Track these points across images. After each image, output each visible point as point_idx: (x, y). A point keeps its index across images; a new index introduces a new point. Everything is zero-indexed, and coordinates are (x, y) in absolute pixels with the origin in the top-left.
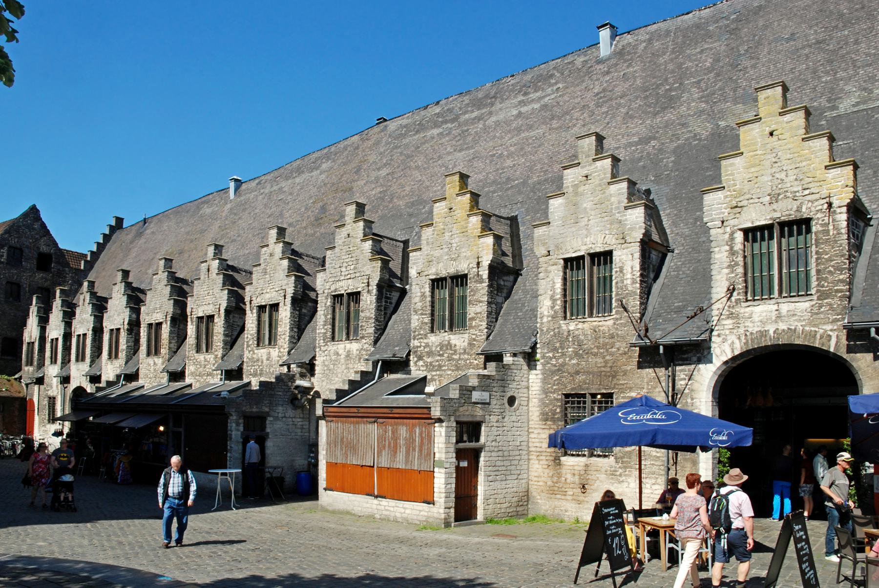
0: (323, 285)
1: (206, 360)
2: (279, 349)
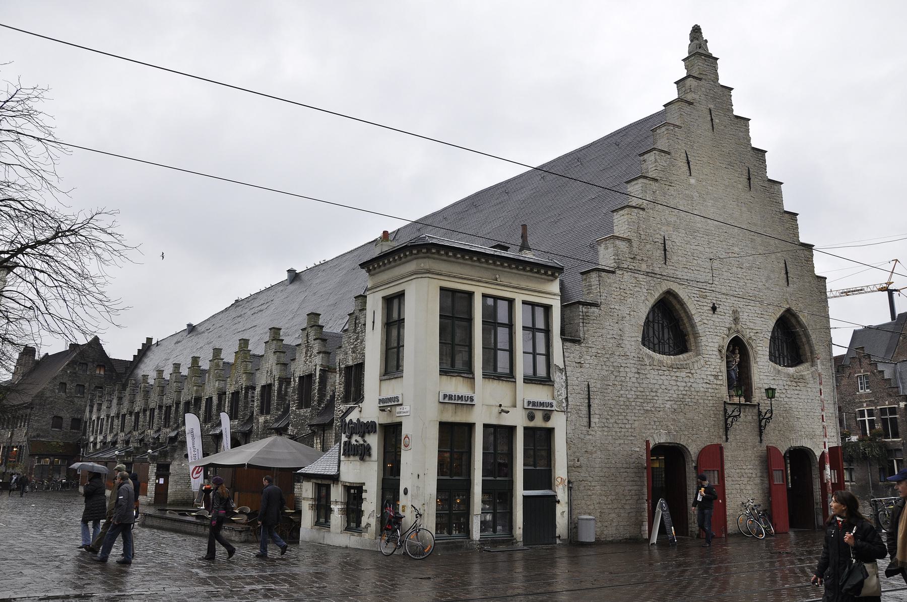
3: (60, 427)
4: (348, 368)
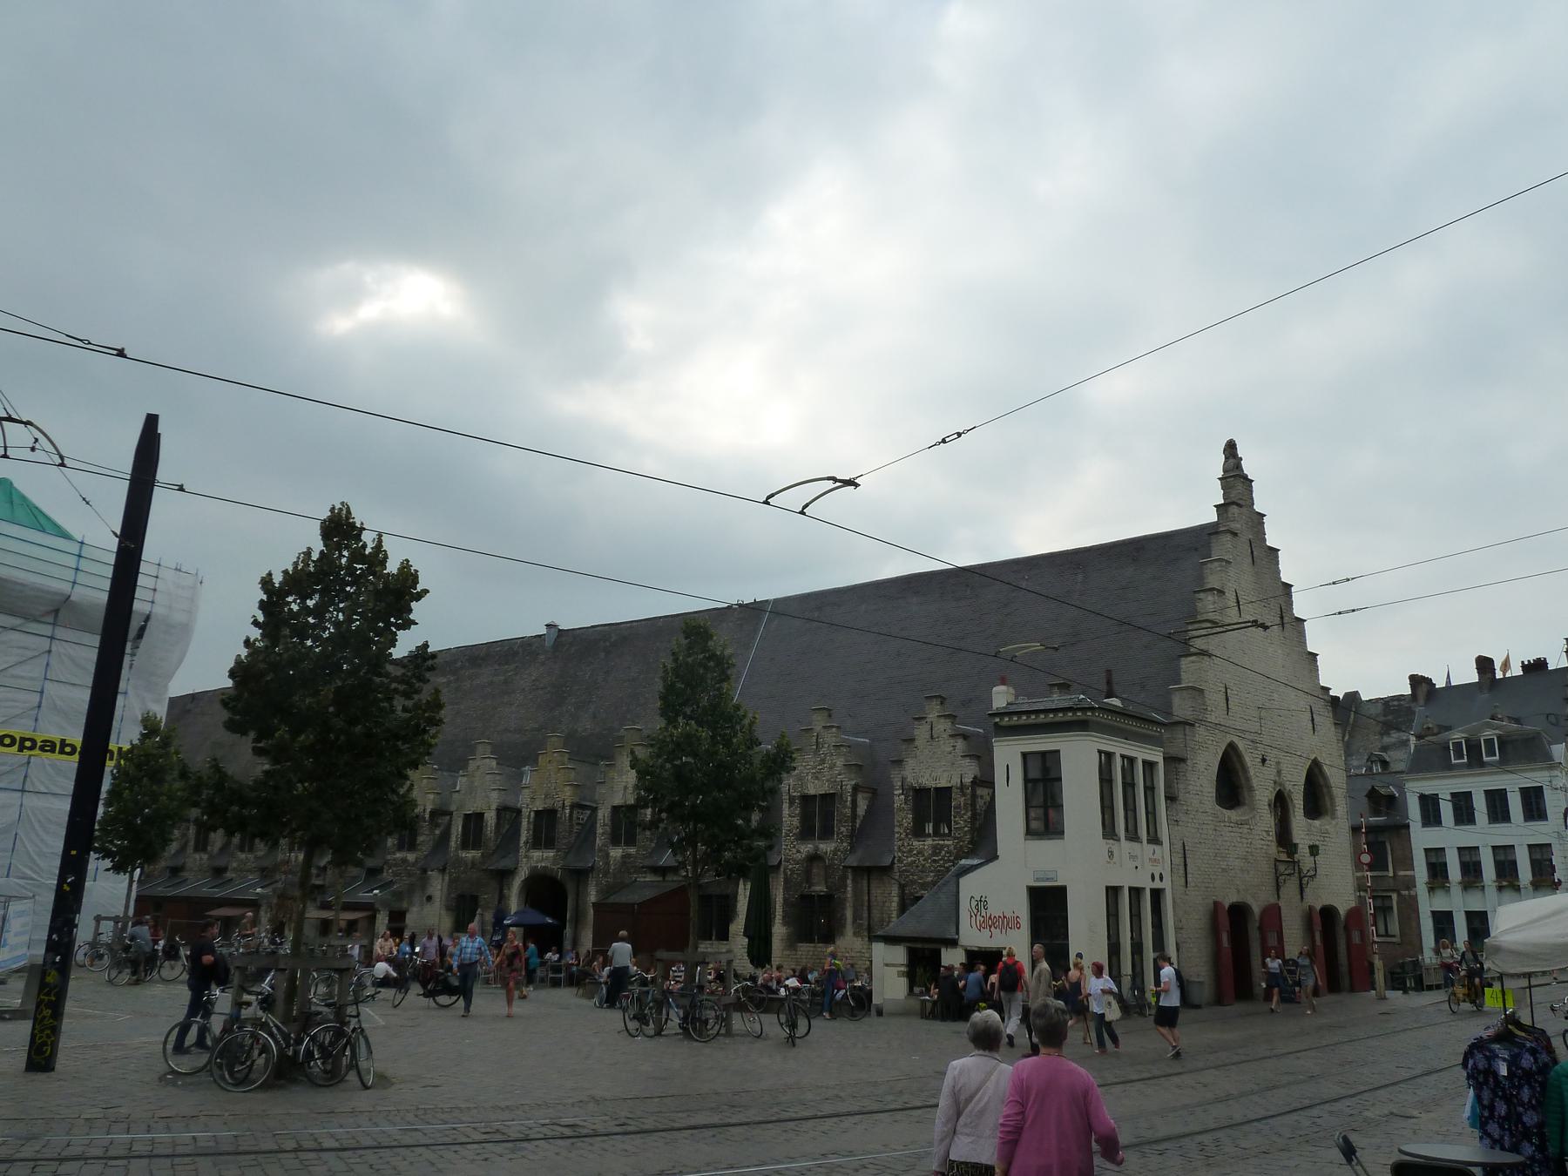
1: (247, 858)
4: (806, 800)
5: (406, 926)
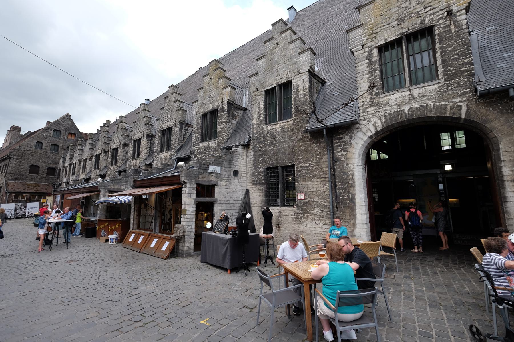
0: (158, 126)
2: (140, 159)
3: (37, 173)
5: (216, 201)
